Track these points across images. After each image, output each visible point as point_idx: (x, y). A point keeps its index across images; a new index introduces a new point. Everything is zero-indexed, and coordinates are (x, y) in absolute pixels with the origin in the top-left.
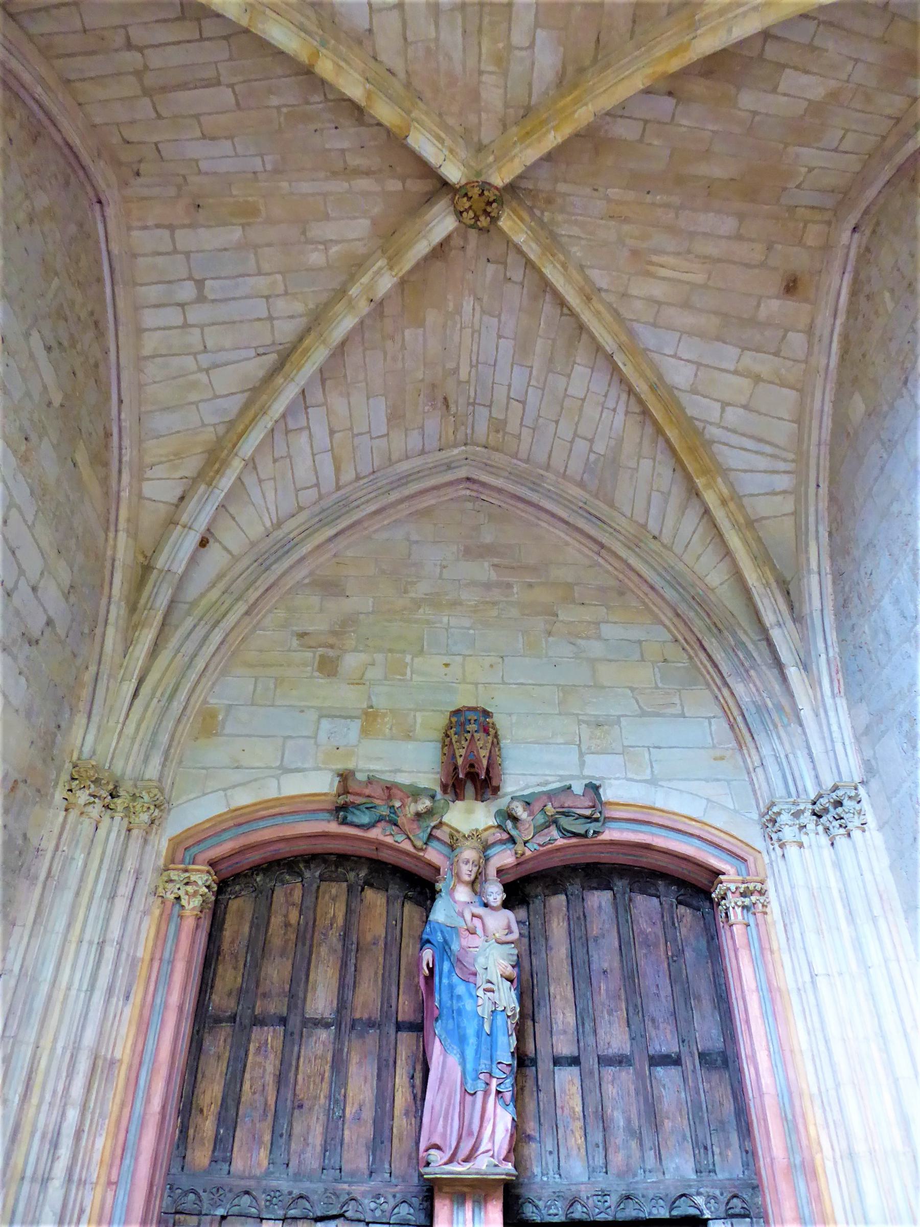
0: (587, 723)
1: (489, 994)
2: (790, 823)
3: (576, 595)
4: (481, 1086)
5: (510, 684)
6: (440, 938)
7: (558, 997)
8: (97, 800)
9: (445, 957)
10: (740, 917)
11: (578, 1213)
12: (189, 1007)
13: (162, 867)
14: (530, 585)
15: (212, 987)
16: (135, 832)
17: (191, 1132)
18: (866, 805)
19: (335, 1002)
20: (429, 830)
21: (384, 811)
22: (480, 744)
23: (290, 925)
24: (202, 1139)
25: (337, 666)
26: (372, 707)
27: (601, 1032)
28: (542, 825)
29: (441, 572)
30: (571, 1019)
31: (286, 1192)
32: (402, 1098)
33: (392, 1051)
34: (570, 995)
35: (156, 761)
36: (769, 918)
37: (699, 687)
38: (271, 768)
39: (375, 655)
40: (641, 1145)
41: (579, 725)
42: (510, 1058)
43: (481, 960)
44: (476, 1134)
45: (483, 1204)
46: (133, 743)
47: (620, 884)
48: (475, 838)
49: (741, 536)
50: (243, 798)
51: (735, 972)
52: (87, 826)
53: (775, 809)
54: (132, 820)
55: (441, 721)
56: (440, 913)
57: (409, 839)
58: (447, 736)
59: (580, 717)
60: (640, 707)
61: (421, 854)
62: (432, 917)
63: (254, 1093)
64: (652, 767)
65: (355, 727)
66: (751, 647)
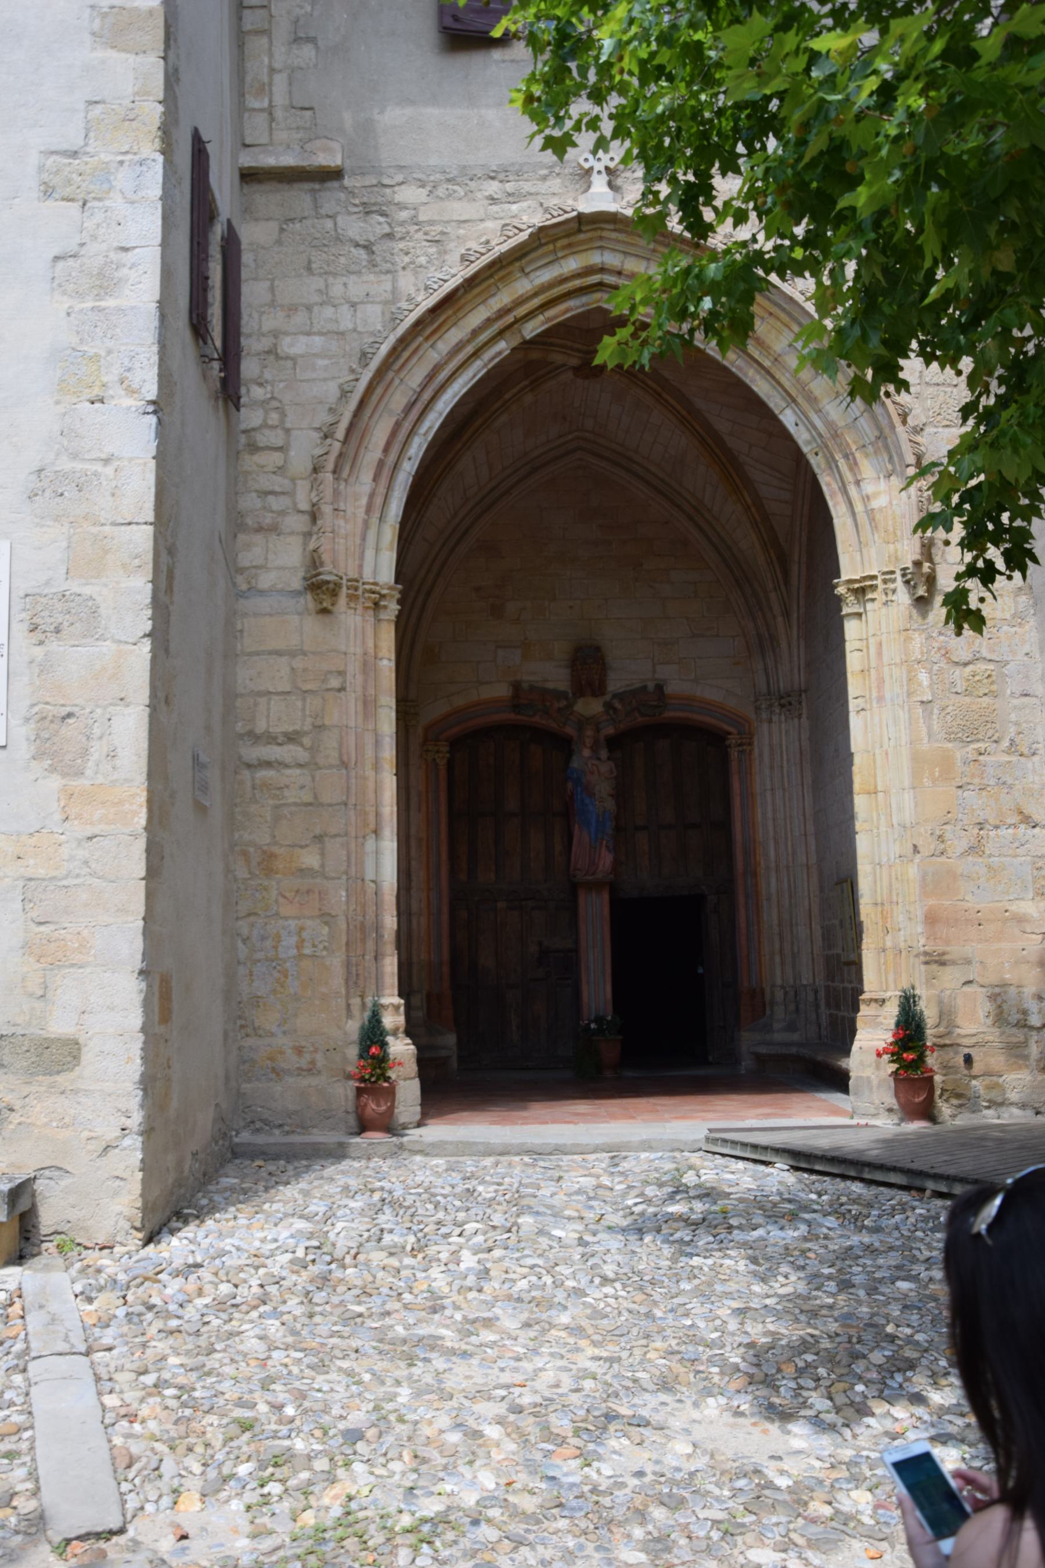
18: (804, 704)
50: (460, 702)
56: (575, 763)
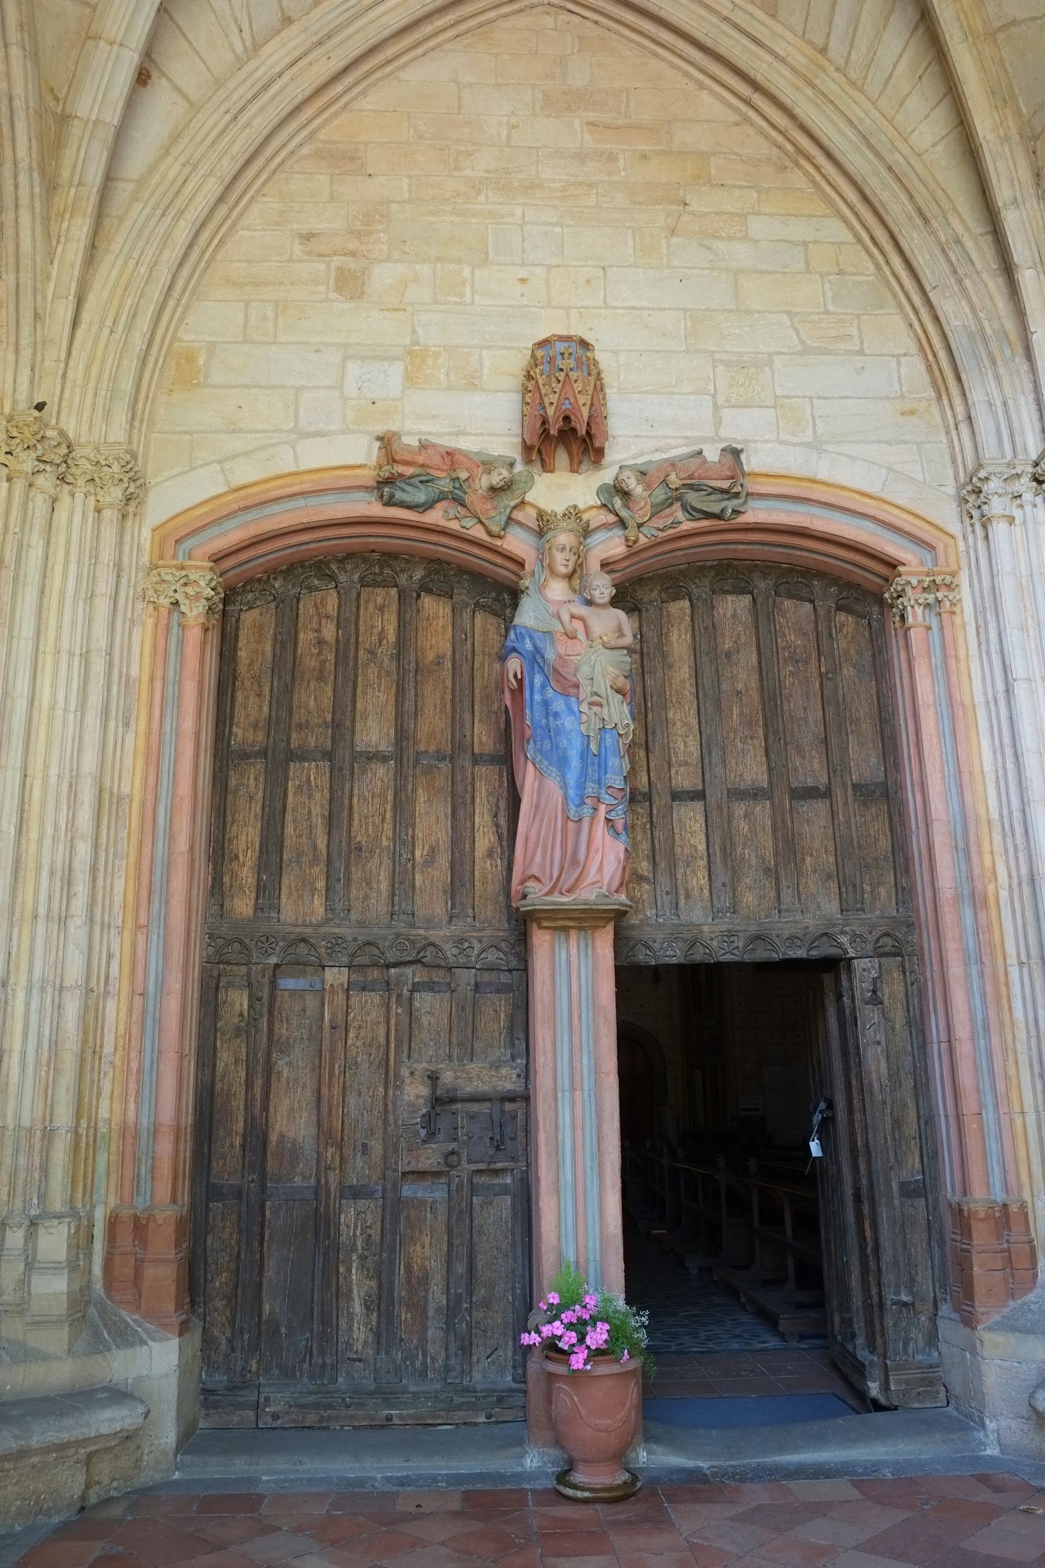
0: (727, 364)
1: (595, 709)
2: (1000, 491)
3: (713, 172)
4: (587, 811)
5: (615, 308)
6: (528, 645)
7: (679, 724)
8: (48, 468)
9: (536, 668)
10: (920, 619)
11: (699, 955)
12: (207, 738)
13: (148, 564)
14: (644, 157)
15: (232, 718)
16: (107, 513)
17: (226, 879)
19: (392, 732)
20: (508, 510)
21: (445, 485)
22: (578, 386)
23: (326, 642)
24: (241, 887)
25: (363, 284)
26: (417, 343)
27: (732, 762)
28: (662, 503)
29: (509, 136)
30: (694, 747)
31: (350, 938)
32: (484, 839)
33: (469, 788)
34: (694, 722)
35: (121, 416)
36: (957, 620)
37: (887, 311)
38: (282, 431)
39: (417, 267)
40: (777, 885)
41: (714, 367)
42: (623, 782)
43: (585, 670)
44: (582, 863)
45: (589, 936)
46: (84, 393)
47: (762, 585)
48: (573, 518)
49: (975, 53)
50: (246, 473)
51: (907, 688)
52: (39, 504)
53: (982, 474)
54: (100, 498)
55: (517, 361)
56: (528, 615)
57: (481, 522)
58: (529, 377)
59: (717, 356)
60: (801, 341)
61: (498, 543)
62: (517, 621)
63: (300, 836)
64: (814, 425)
65: (397, 371)
66: (969, 244)
